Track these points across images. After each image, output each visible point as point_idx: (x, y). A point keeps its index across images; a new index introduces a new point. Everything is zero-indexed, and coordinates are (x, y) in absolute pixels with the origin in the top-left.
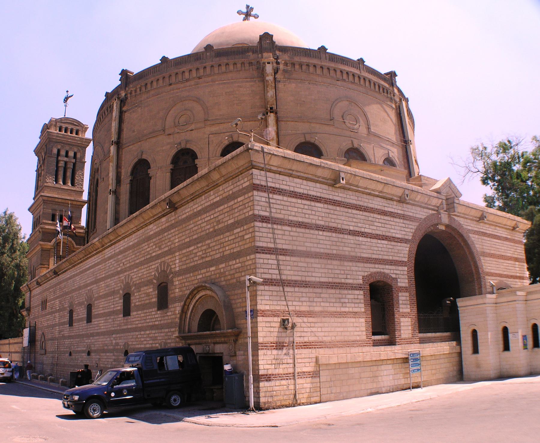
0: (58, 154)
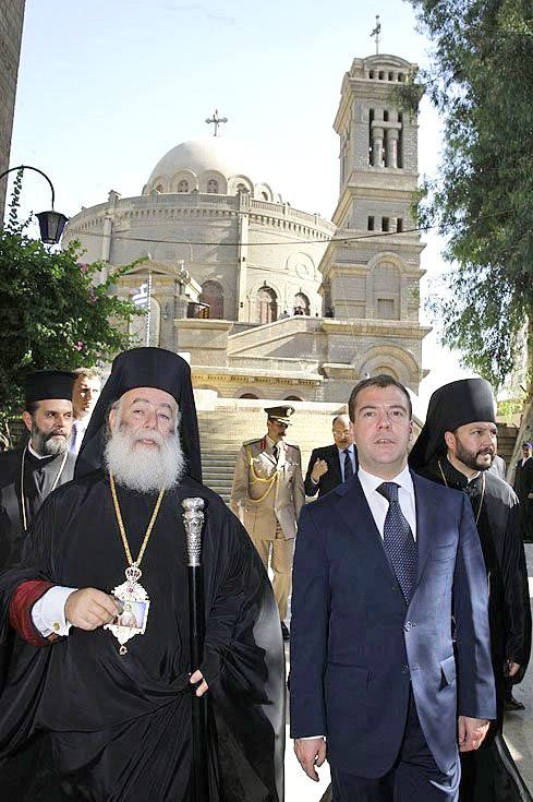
0: (372, 118)
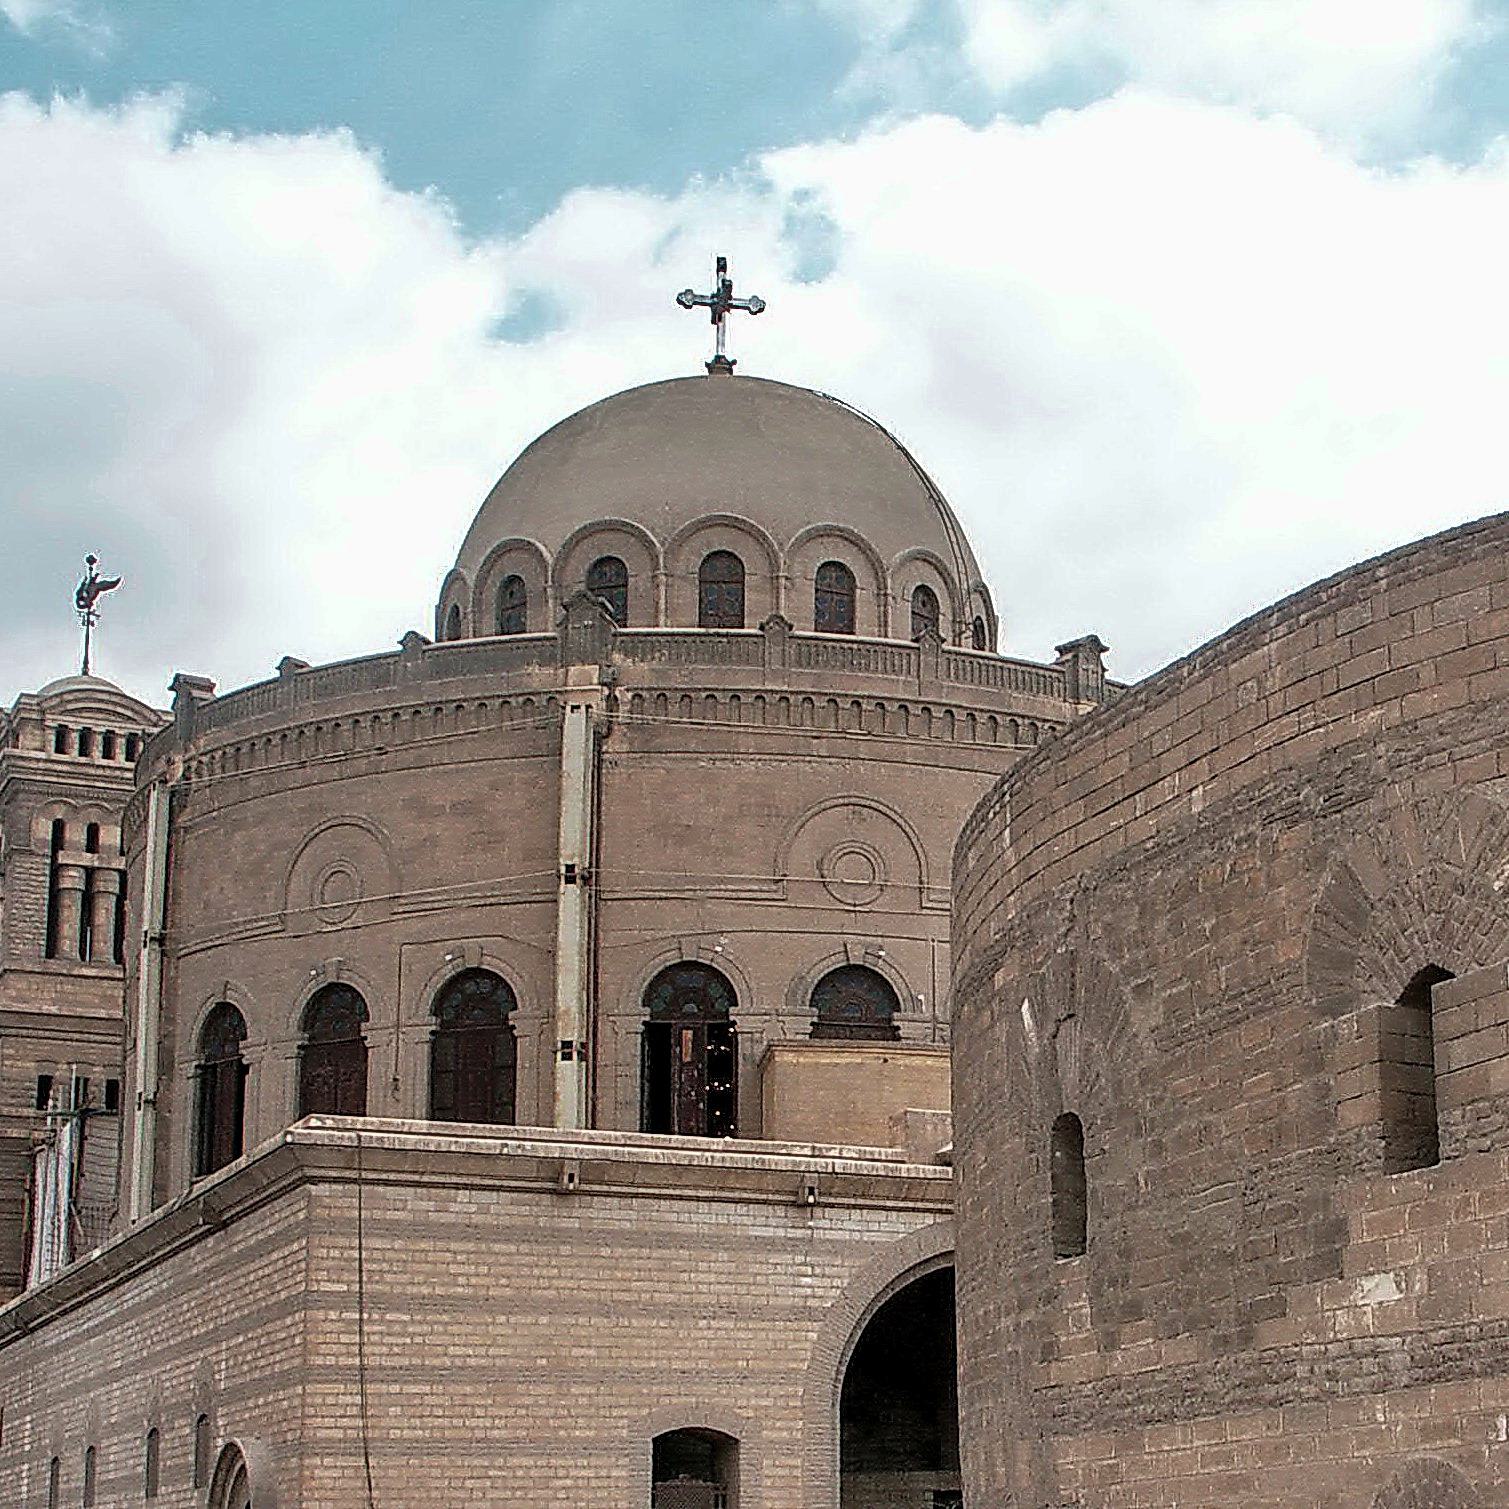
0: (58, 842)
